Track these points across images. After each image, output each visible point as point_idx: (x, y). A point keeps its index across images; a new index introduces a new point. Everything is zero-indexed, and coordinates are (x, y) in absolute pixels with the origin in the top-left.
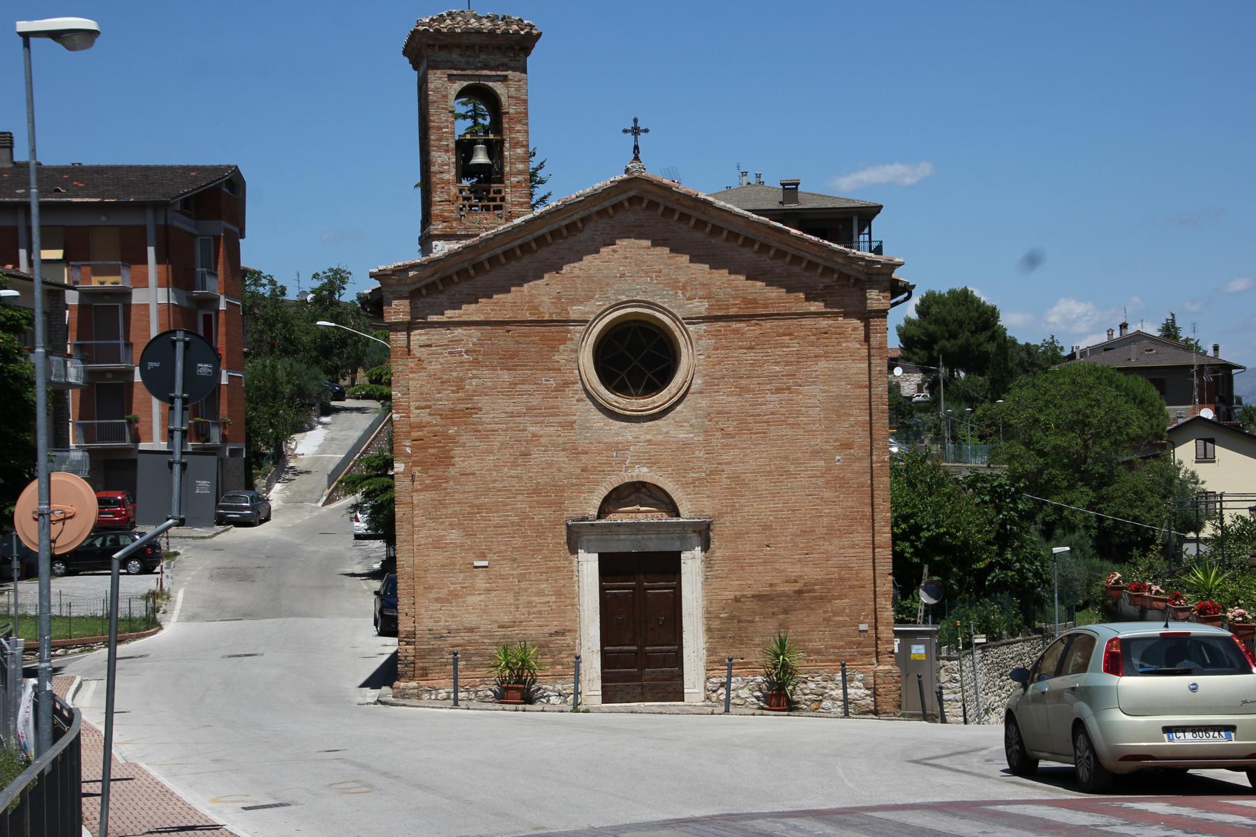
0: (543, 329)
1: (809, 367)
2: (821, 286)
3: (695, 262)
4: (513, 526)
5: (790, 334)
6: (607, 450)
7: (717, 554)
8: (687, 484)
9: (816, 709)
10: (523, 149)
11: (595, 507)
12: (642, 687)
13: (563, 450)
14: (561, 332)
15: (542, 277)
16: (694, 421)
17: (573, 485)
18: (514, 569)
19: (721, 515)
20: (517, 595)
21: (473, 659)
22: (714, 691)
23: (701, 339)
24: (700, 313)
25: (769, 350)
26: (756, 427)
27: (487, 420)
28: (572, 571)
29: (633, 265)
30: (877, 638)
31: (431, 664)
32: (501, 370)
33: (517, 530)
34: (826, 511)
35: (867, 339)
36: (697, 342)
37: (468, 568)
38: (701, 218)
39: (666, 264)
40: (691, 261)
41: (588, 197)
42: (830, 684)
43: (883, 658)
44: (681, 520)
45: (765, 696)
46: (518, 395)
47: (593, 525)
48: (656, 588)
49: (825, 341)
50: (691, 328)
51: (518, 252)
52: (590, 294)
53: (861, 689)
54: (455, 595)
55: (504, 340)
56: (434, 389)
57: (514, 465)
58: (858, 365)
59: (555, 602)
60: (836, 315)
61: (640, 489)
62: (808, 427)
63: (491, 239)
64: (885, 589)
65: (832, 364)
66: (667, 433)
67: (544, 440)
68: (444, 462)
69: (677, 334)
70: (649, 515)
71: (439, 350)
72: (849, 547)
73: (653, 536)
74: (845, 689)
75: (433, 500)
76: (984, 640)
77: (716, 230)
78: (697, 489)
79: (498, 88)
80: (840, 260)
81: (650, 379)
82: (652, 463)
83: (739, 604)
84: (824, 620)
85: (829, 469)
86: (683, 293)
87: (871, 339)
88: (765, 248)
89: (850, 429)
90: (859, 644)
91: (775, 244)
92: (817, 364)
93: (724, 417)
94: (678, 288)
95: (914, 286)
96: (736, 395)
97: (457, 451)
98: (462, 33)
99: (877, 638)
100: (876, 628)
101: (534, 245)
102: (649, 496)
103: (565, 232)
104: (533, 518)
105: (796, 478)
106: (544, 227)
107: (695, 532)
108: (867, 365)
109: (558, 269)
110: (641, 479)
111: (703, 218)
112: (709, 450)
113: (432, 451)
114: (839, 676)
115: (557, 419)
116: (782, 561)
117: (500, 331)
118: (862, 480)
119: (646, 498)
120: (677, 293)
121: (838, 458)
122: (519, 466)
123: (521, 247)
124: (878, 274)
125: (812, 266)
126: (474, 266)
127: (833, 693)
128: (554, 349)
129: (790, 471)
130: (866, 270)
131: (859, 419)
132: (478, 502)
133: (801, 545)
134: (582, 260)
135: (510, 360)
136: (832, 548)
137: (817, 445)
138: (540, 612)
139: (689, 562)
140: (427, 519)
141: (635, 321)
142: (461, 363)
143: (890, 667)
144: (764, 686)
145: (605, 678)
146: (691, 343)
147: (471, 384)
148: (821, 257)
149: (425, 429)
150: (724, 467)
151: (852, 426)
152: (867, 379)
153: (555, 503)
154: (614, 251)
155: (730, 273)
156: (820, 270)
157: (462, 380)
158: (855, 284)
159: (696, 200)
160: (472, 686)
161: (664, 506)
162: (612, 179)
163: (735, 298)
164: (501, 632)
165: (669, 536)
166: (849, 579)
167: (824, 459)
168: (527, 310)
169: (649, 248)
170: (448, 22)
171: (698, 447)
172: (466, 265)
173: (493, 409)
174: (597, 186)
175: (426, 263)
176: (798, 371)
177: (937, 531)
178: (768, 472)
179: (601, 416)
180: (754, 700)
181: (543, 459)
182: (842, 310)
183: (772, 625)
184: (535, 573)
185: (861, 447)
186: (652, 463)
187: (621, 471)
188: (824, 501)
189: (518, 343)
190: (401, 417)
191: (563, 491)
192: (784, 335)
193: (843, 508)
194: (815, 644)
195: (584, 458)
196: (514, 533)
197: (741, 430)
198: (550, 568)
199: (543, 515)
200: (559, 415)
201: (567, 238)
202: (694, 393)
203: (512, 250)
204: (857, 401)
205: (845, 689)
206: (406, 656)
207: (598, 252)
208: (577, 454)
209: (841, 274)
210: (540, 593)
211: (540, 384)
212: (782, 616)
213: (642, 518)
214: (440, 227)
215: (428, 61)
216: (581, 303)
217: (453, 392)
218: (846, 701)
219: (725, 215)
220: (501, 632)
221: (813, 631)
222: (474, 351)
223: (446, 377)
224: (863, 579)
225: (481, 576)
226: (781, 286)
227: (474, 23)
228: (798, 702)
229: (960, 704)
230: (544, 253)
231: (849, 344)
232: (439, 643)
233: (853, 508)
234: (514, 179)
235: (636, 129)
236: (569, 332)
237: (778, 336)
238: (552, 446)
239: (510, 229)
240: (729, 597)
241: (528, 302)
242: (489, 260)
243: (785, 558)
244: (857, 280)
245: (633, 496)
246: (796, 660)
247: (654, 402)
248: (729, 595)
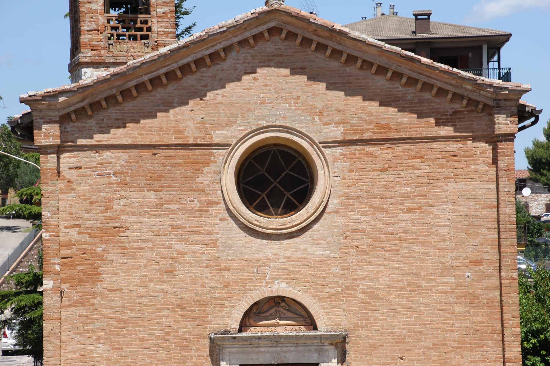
6: (248, 266)
44: (318, 333)
61: (279, 303)
70: (288, 328)
73: (292, 349)
102: (288, 310)
119: (285, 311)
161: (302, 319)
165: (307, 348)
187: (261, 286)
208: (220, 270)
245: (273, 310)
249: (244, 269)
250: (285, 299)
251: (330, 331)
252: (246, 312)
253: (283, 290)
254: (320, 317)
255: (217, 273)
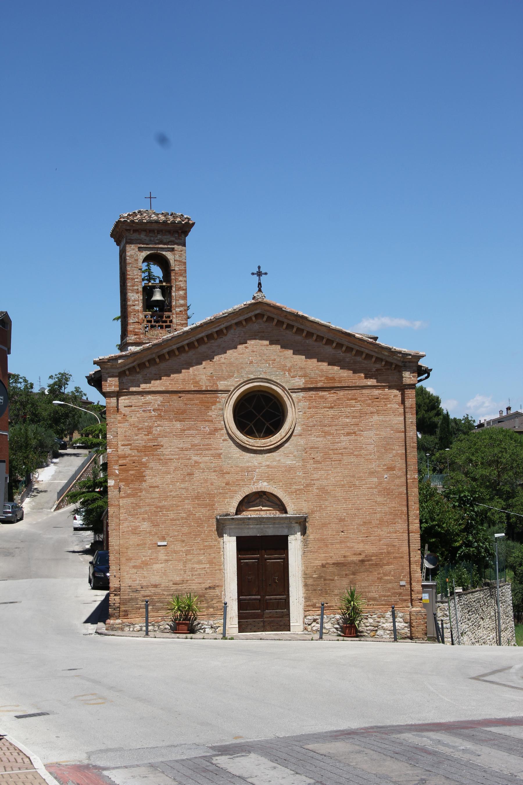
0: (202, 396)
1: (367, 419)
2: (374, 369)
3: (296, 355)
4: (182, 520)
5: (356, 399)
6: (241, 471)
7: (311, 537)
8: (292, 492)
9: (373, 636)
10: (184, 291)
11: (234, 508)
12: (264, 622)
13: (214, 472)
14: (213, 398)
15: (202, 364)
16: (296, 453)
17: (220, 493)
18: (183, 547)
19: (313, 512)
20: (185, 563)
21: (157, 604)
22: (309, 625)
23: (300, 402)
24: (300, 386)
25: (343, 409)
26: (335, 457)
27: (167, 453)
28: (220, 548)
29: (258, 356)
30: (412, 590)
31: (130, 608)
32: (175, 421)
33: (185, 522)
34: (378, 510)
35: (403, 402)
36: (298, 404)
37: (154, 546)
38: (300, 327)
39: (278, 356)
40: (294, 354)
41: (230, 314)
42: (382, 620)
43: (416, 603)
44: (288, 515)
45: (341, 627)
46: (186, 437)
47: (233, 519)
48: (272, 559)
49: (377, 403)
50: (294, 395)
51: (186, 348)
52: (231, 374)
53: (401, 622)
54: (145, 564)
55: (176, 402)
56: (133, 433)
57: (183, 481)
58: (398, 419)
59: (209, 568)
60: (384, 387)
61: (262, 496)
62: (367, 457)
63: (170, 340)
64: (416, 559)
65: (381, 418)
66: (279, 460)
67: (202, 465)
68: (139, 479)
69: (286, 399)
70: (268, 512)
71: (137, 409)
72: (393, 532)
73: (271, 526)
74: (394, 622)
75: (132, 503)
76: (461, 591)
77: (310, 335)
78: (298, 496)
79: (169, 255)
80: (386, 354)
81: (268, 427)
82: (269, 480)
83: (325, 569)
84: (378, 578)
85: (380, 483)
86: (289, 374)
87: (406, 402)
88: (339, 346)
89: (393, 458)
90: (400, 594)
91: (346, 343)
92: (372, 418)
93: (315, 451)
94: (286, 370)
95: (431, 370)
96: (322, 437)
97: (148, 472)
98: (147, 222)
99: (412, 590)
100: (411, 584)
101: (196, 344)
102: (268, 501)
103: (215, 336)
104: (195, 515)
105: (360, 489)
106: (202, 332)
107: (297, 523)
108: (403, 418)
109: (211, 359)
110: (263, 490)
111: (302, 327)
112: (305, 471)
113: (132, 472)
114: (389, 614)
115: (210, 452)
116: (351, 541)
117: (175, 397)
118: (401, 490)
119: (266, 501)
120: (285, 373)
121: (386, 476)
122: (186, 481)
123: (188, 344)
124: (409, 362)
125: (368, 357)
126: (159, 357)
127: (384, 625)
128: (208, 408)
129: (356, 484)
130: (402, 360)
131: (399, 452)
132: (160, 504)
133: (363, 531)
134: (226, 353)
135: (181, 415)
136: (383, 533)
137: (373, 468)
138: (199, 574)
139: (293, 542)
140: (128, 515)
141: (259, 391)
142: (150, 417)
143: (419, 609)
144: (341, 621)
145: (240, 617)
146: (294, 404)
147: (156, 430)
148: (375, 352)
149: (128, 459)
150: (315, 482)
151: (394, 456)
152: (404, 427)
153: (209, 505)
154: (246, 347)
155: (318, 361)
156: (374, 359)
157: (151, 427)
158: (395, 369)
159: (297, 316)
160: (156, 622)
161: (277, 506)
162: (245, 303)
163: (321, 377)
164: (175, 587)
165: (281, 525)
166: (393, 553)
167: (377, 477)
168: (192, 384)
169: (267, 346)
170: (139, 216)
171: (299, 469)
172: (154, 356)
173: (170, 446)
174: (236, 307)
175: (129, 354)
176: (360, 422)
177: (432, 524)
178: (342, 485)
179: (238, 450)
180: (335, 630)
181: (202, 477)
182: (387, 384)
183: (345, 582)
184: (196, 549)
185: (400, 469)
186: (270, 479)
187: (250, 485)
188: (377, 504)
189: (186, 404)
190: (113, 451)
191: (214, 497)
192: (352, 399)
193: (389, 508)
194: (372, 594)
195: (227, 476)
196: (183, 524)
197: (326, 459)
198: (206, 546)
199: (201, 512)
200: (211, 450)
201: (216, 339)
202: (296, 436)
203: (183, 347)
204: (398, 440)
205: (394, 622)
206: (114, 603)
207: (236, 348)
208: (223, 474)
209: (387, 362)
210: (200, 562)
211: (200, 430)
212: (352, 576)
213: (263, 514)
214: (133, 338)
215: (126, 239)
216: (225, 379)
217: (145, 435)
218: (395, 630)
219: (315, 325)
220: (175, 587)
221: (371, 586)
222: (159, 410)
223: (141, 426)
224: (402, 553)
225: (162, 552)
226: (349, 369)
227: (154, 217)
228: (362, 632)
229: (449, 630)
230: (203, 349)
231: (392, 406)
232: (135, 594)
233: (396, 508)
234: (178, 310)
235: (259, 273)
236: (218, 397)
237: (347, 400)
238: (208, 469)
239: (182, 333)
240: (318, 564)
241: (193, 379)
242: (169, 353)
243: (353, 539)
244: (397, 366)
245: (258, 501)
246: (361, 604)
247: (271, 441)
248: (319, 563)
249: (239, 474)
250: (266, 493)
251: (296, 514)
252: (240, 502)
253: (265, 487)
254: (289, 505)
255: (221, 476)
